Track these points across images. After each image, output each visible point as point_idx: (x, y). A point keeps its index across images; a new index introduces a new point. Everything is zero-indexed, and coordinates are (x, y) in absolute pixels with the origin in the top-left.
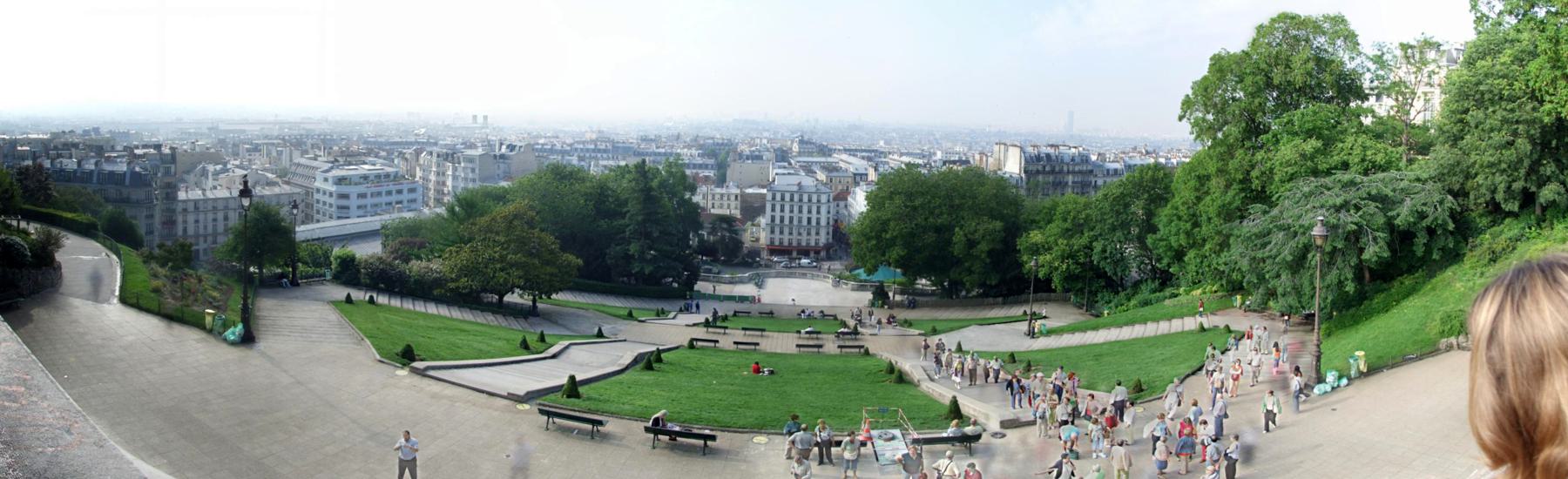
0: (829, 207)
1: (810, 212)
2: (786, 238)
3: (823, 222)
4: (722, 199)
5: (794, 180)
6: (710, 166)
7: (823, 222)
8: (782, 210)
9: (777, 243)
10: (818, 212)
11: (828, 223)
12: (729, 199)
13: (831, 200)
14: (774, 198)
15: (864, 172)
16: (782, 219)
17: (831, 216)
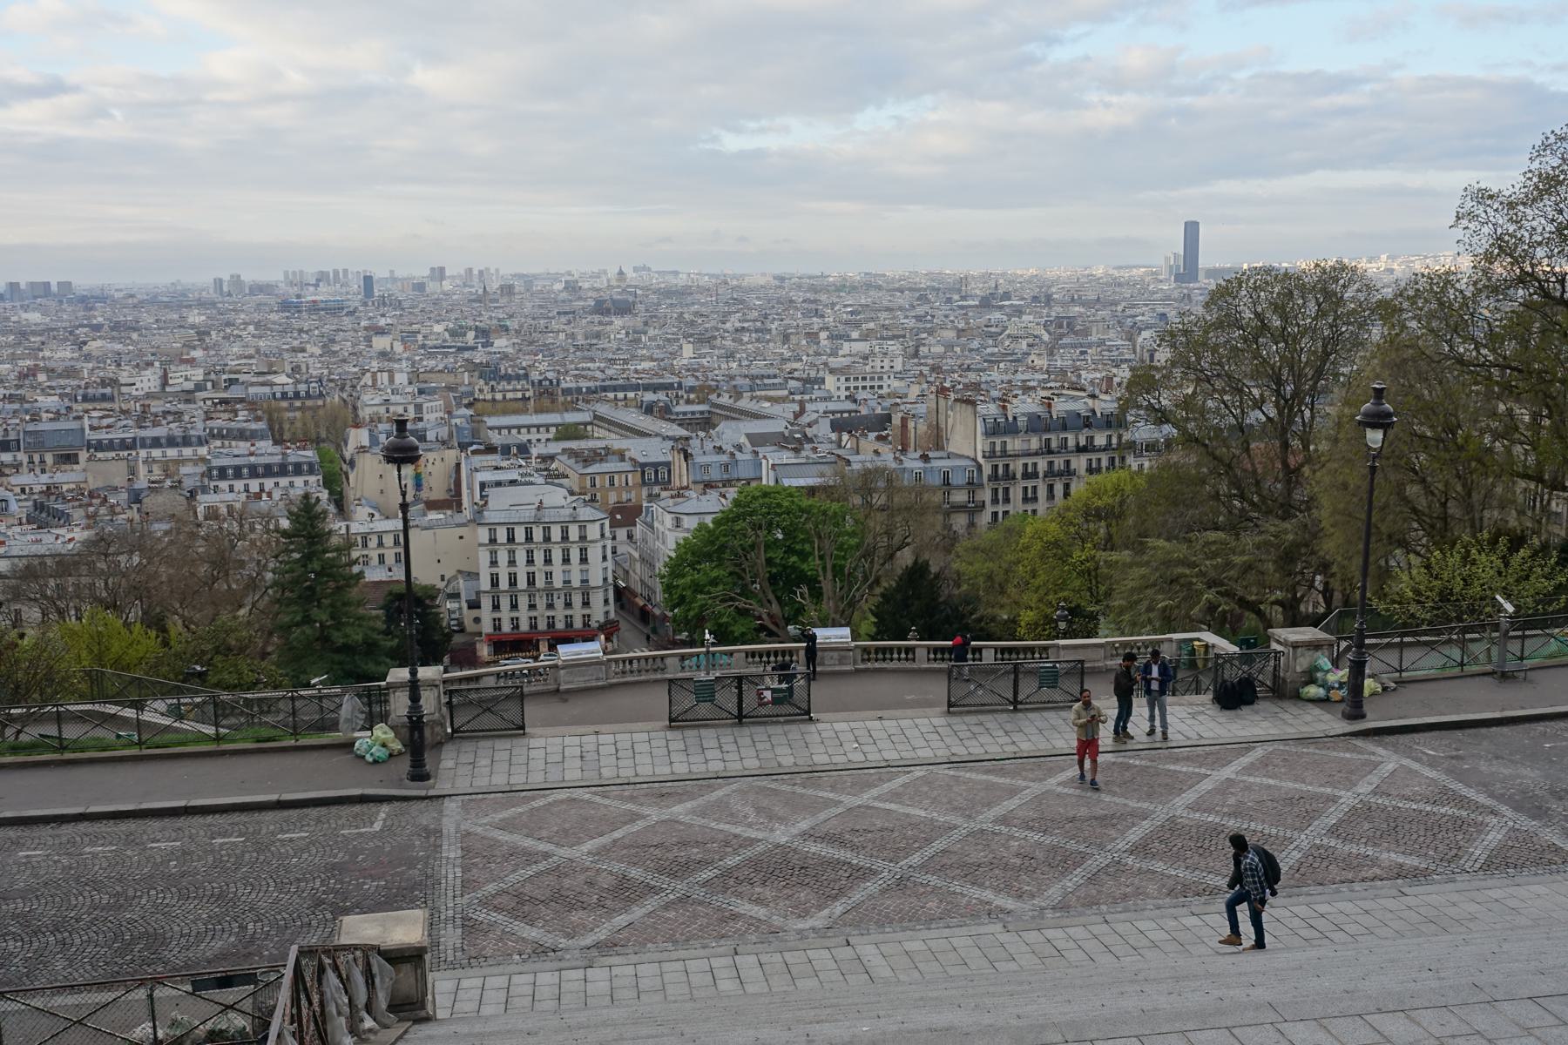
0: (604, 547)
1: (566, 560)
2: (524, 615)
3: (596, 580)
4: (365, 545)
5: (527, 495)
6: (305, 467)
7: (596, 580)
8: (512, 562)
9: (506, 627)
10: (584, 560)
11: (605, 579)
12: (381, 544)
13: (608, 534)
14: (493, 541)
15: (662, 459)
16: (513, 582)
17: (610, 564)
